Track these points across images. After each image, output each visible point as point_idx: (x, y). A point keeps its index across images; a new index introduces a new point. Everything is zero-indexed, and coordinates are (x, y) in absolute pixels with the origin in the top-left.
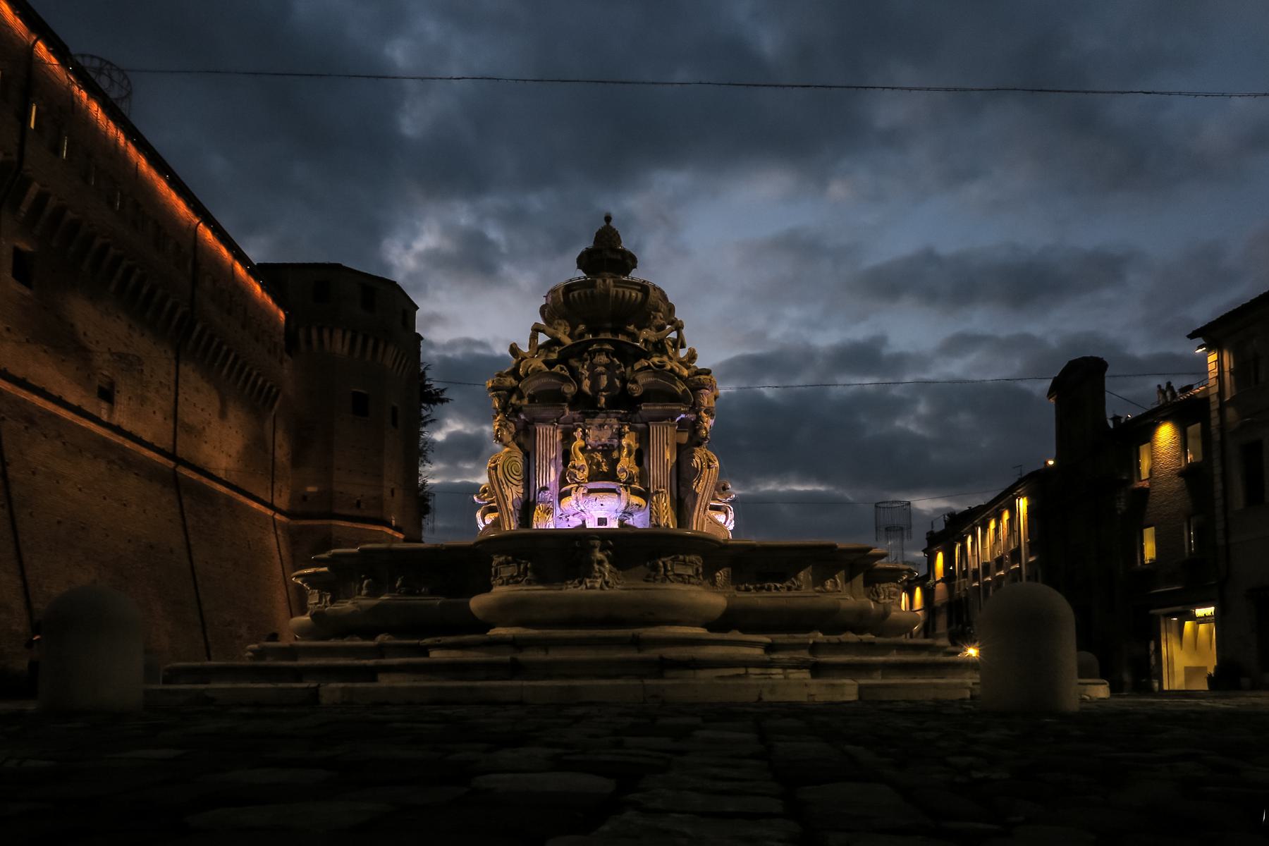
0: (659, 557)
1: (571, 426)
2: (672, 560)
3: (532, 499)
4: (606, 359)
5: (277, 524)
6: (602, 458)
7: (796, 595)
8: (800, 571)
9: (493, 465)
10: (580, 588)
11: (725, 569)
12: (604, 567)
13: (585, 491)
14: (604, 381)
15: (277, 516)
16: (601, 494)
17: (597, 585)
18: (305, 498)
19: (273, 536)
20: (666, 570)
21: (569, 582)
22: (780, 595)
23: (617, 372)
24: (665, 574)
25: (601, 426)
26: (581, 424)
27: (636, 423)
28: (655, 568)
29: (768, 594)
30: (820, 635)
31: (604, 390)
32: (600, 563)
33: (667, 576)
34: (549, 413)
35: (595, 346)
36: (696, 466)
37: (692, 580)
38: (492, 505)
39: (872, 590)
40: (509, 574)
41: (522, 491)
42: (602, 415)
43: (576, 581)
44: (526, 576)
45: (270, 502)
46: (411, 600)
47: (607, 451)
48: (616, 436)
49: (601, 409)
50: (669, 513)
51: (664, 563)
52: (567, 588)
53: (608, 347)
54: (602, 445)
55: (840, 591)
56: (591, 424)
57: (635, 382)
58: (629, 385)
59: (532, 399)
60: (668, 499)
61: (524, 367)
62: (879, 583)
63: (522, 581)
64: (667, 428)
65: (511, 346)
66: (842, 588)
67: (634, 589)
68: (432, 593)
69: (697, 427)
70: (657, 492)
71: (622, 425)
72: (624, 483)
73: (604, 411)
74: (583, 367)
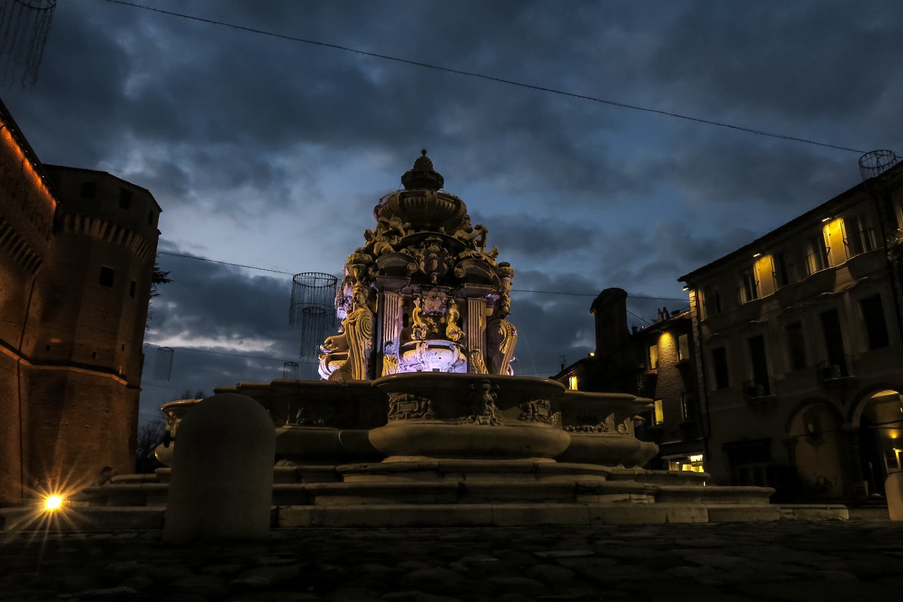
1: (411, 296)
2: (537, 403)
3: (378, 350)
4: (438, 248)
5: (21, 367)
7: (592, 435)
8: (606, 417)
11: (557, 413)
12: (492, 406)
13: (427, 347)
14: (435, 264)
15: (22, 361)
16: (440, 350)
17: (488, 421)
18: (48, 348)
19: (16, 377)
20: (534, 412)
21: (462, 418)
23: (446, 258)
24: (533, 415)
25: (434, 298)
26: (419, 294)
28: (526, 409)
29: (586, 434)
31: (435, 271)
32: (489, 403)
34: (395, 284)
35: (430, 238)
38: (334, 354)
40: (411, 410)
41: (371, 344)
42: (435, 289)
43: (470, 417)
44: (426, 411)
45: (18, 349)
46: (310, 429)
47: (436, 316)
48: (445, 306)
49: (434, 285)
51: (532, 405)
52: (461, 423)
55: (628, 434)
56: (426, 295)
58: (456, 269)
60: (482, 357)
63: (422, 415)
64: (480, 303)
65: (367, 231)
68: (328, 424)
69: (503, 304)
70: (475, 351)
71: (448, 298)
72: (455, 342)
73: (437, 286)
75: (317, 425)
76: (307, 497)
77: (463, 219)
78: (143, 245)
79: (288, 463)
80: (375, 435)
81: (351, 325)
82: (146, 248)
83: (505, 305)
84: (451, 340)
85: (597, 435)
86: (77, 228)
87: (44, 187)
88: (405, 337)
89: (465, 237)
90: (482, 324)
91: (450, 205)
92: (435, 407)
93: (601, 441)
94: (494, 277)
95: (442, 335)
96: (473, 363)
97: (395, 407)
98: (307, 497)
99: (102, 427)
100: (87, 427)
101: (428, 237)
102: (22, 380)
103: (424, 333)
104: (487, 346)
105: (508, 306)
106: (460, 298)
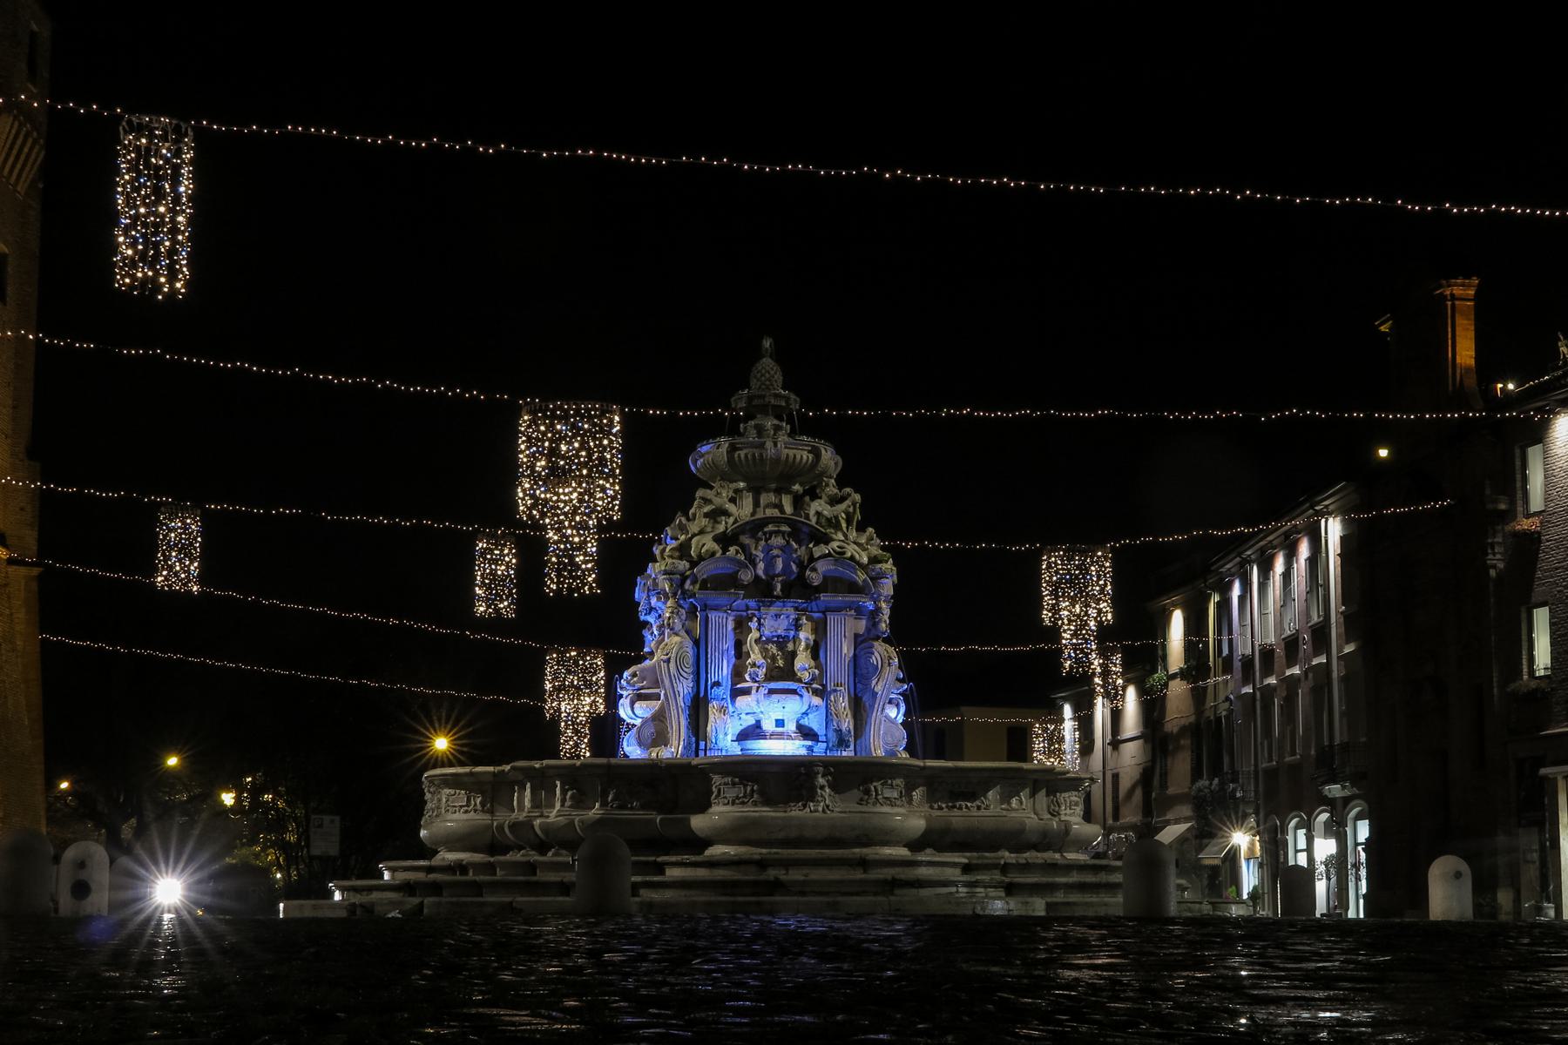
0: (872, 782)
3: (702, 695)
4: (783, 541)
6: (778, 651)
9: (666, 657)
10: (805, 811)
11: (921, 788)
12: (825, 791)
13: (766, 692)
16: (784, 696)
17: (820, 809)
20: (877, 794)
21: (792, 804)
23: (795, 556)
25: (777, 616)
26: (756, 612)
27: (811, 612)
28: (867, 792)
30: (1007, 854)
31: (778, 575)
32: (822, 788)
33: (878, 800)
35: (770, 528)
36: (875, 663)
37: (898, 803)
38: (642, 691)
39: (1052, 801)
41: (691, 685)
43: (800, 804)
47: (781, 642)
48: (793, 628)
49: (778, 597)
50: (849, 716)
51: (875, 787)
53: (785, 528)
54: (776, 636)
56: (766, 614)
57: (814, 570)
58: (808, 572)
59: (704, 586)
60: (846, 698)
61: (696, 547)
62: (1061, 792)
66: (1026, 806)
67: (850, 812)
68: (643, 807)
70: (835, 691)
72: (805, 683)
74: (756, 548)
75: (632, 808)
77: (825, 479)
78: (19, 142)
80: (698, 822)
81: (664, 662)
82: (26, 150)
83: (880, 621)
84: (800, 680)
85: (975, 814)
88: (737, 674)
89: (825, 513)
90: (847, 649)
91: (805, 457)
92: (761, 793)
94: (864, 581)
95: (788, 673)
96: (832, 708)
97: (719, 791)
101: (766, 525)
103: (762, 672)
104: (855, 680)
105: (885, 621)
106: (814, 612)
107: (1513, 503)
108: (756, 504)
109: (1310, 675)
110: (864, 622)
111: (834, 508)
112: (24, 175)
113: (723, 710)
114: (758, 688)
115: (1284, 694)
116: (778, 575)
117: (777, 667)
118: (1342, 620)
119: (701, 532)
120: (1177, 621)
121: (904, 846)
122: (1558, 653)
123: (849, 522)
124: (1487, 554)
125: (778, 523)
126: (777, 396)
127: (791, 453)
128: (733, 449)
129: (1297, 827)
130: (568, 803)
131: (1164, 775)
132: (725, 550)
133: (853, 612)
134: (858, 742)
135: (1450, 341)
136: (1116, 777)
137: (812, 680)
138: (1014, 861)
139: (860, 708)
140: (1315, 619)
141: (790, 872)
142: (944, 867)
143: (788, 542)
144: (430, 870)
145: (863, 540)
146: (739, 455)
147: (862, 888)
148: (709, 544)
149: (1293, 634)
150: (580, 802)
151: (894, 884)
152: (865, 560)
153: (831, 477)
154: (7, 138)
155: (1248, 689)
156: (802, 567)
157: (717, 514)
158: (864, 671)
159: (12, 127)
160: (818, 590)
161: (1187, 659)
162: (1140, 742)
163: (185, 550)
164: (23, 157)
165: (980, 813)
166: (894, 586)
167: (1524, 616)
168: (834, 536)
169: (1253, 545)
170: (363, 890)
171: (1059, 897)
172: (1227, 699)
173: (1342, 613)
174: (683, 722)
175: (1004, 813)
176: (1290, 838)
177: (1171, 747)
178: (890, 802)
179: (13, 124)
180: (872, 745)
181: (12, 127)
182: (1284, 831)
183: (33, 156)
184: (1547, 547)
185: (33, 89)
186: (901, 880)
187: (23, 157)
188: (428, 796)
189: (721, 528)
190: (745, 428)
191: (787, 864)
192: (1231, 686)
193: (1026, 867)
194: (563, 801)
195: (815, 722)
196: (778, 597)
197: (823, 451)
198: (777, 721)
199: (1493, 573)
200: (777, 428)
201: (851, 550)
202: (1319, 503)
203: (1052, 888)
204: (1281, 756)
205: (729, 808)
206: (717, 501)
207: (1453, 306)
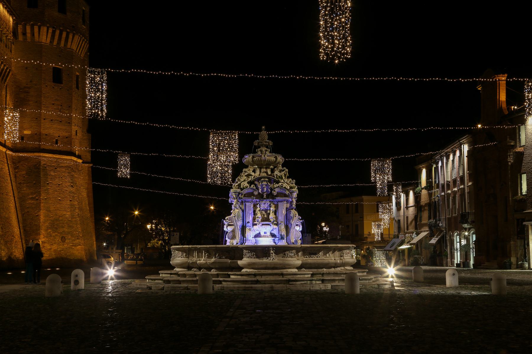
3: (244, 225)
5: (8, 155)
8: (319, 253)
13: (261, 225)
16: (266, 226)
17: (272, 259)
19: (6, 165)
20: (287, 255)
22: (315, 259)
23: (269, 187)
25: (265, 204)
28: (285, 254)
29: (312, 259)
32: (272, 253)
34: (250, 200)
35: (263, 179)
38: (229, 224)
41: (242, 223)
47: (266, 211)
49: (265, 198)
51: (287, 253)
57: (274, 191)
58: (273, 192)
59: (245, 196)
60: (284, 226)
67: (280, 260)
68: (226, 258)
70: (281, 224)
75: (223, 258)
76: (220, 282)
78: (81, 42)
79: (215, 270)
80: (240, 262)
82: (83, 45)
83: (293, 204)
84: (270, 221)
86: (29, 35)
87: (4, 10)
88: (254, 219)
89: (278, 174)
90: (284, 212)
91: (273, 159)
92: (256, 255)
93: (315, 261)
94: (288, 193)
95: (268, 219)
97: (245, 254)
98: (220, 282)
99: (71, 199)
100: (59, 200)
101: (262, 179)
102: (10, 166)
103: (260, 220)
104: (286, 221)
107: (516, 143)
108: (260, 172)
109: (460, 191)
110: (289, 204)
111: (281, 173)
112: (83, 52)
113: (250, 230)
114: (259, 224)
115: (453, 196)
116: (265, 192)
117: (265, 218)
118: (468, 175)
119: (244, 181)
120: (424, 172)
121: (296, 268)
122: (529, 188)
123: (285, 176)
124: (508, 158)
125: (265, 178)
126: (266, 142)
127: (269, 158)
128: (253, 157)
129: (457, 235)
130: (206, 257)
131: (421, 218)
132: (250, 186)
133: (285, 202)
134: (287, 237)
135: (498, 93)
136: (407, 217)
137: (274, 221)
138: (325, 272)
139: (288, 228)
140: (461, 174)
141: (263, 277)
142: (307, 273)
143: (267, 183)
144: (171, 274)
145: (288, 182)
146: (255, 159)
147: (280, 282)
148: (246, 184)
149: (455, 179)
150: (209, 257)
151: (289, 281)
152: (289, 188)
153: (280, 164)
154: (77, 42)
155: (443, 194)
156: (271, 189)
157: (248, 176)
158: (289, 218)
159: (78, 39)
160: (276, 196)
161: (427, 184)
162: (414, 207)
163: (125, 166)
164: (82, 47)
165: (317, 259)
166: (297, 194)
167: (519, 176)
168: (281, 181)
169: (449, 148)
170: (153, 280)
171: (336, 283)
172: (438, 196)
173: (468, 173)
174: (239, 233)
175: (325, 258)
176: (455, 238)
177: (423, 209)
178: (291, 257)
179: (78, 38)
180: (291, 238)
181: (78, 39)
182: (453, 236)
183: (85, 46)
184: (526, 156)
185: (84, 27)
186: (291, 280)
187: (82, 47)
188: (172, 253)
189: (250, 179)
190: (258, 151)
191: (261, 275)
192: (439, 192)
193: (329, 274)
194: (205, 256)
195: (275, 232)
196: (265, 198)
197: (278, 157)
198: (264, 232)
199: (510, 163)
200: (266, 151)
201: (285, 185)
202: (461, 140)
203: (334, 280)
204: (452, 214)
205: (248, 259)
206: (249, 172)
207: (499, 83)
